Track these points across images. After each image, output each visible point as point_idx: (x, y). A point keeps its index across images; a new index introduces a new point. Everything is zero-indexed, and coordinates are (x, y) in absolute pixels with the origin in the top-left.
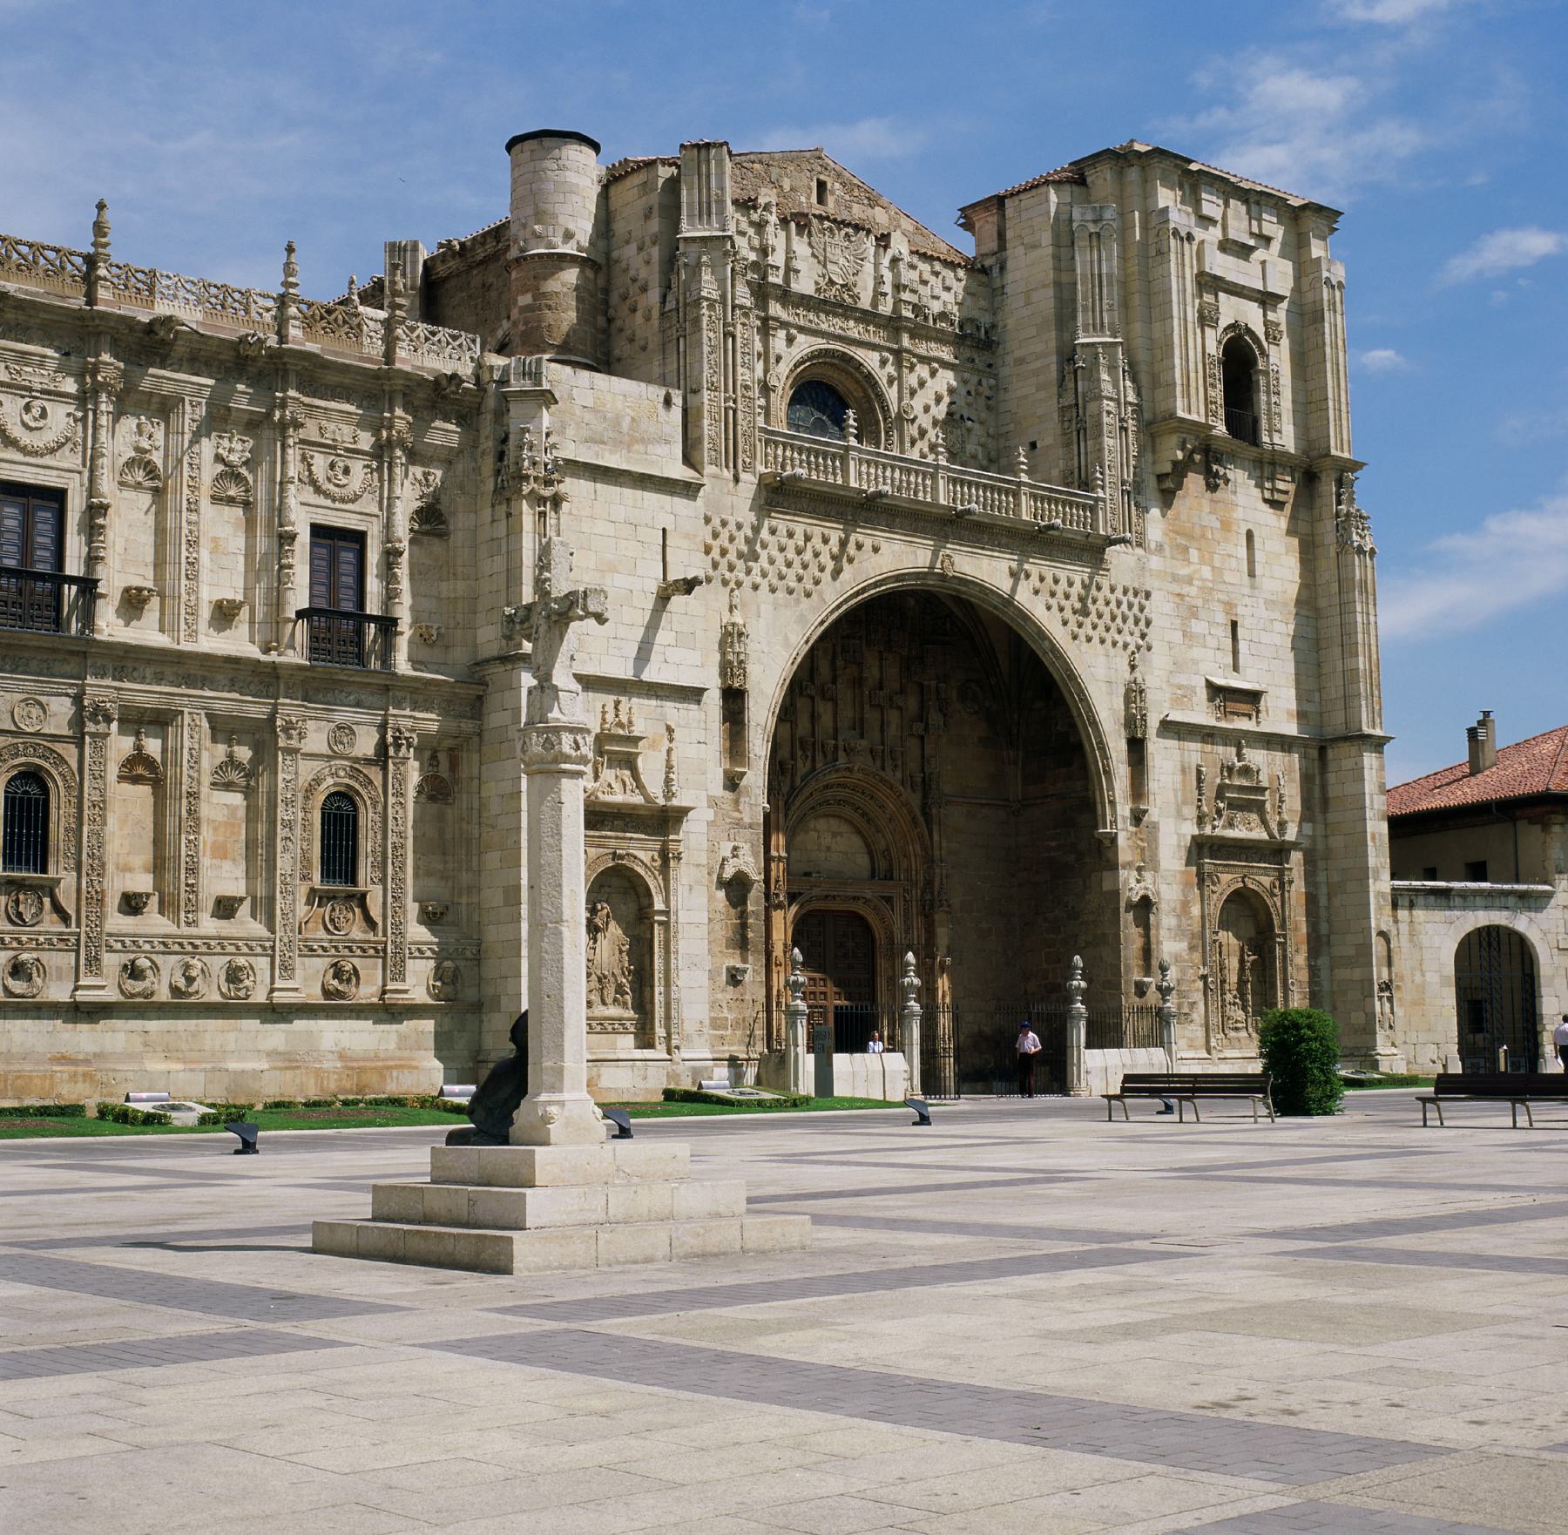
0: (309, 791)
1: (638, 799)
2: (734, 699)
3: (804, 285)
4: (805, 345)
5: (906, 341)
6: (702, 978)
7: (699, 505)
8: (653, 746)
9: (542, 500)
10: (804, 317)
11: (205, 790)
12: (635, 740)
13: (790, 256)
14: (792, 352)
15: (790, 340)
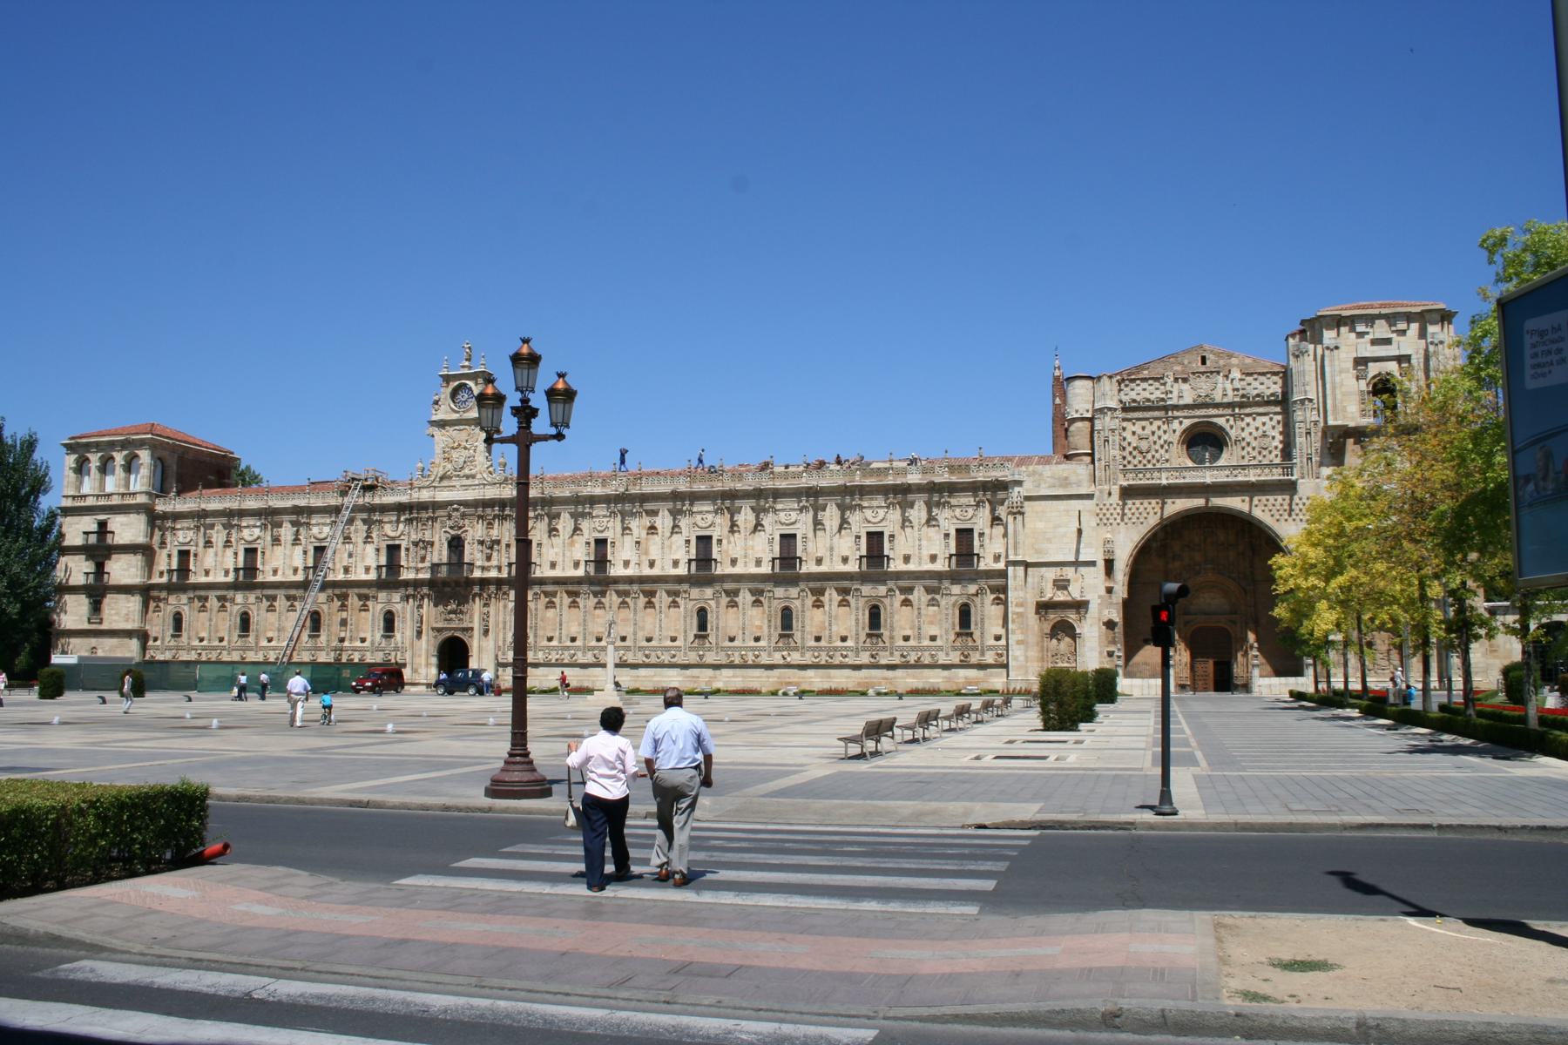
0: (954, 605)
1: (1069, 599)
2: (1109, 565)
3: (1188, 400)
4: (1187, 423)
5: (1237, 410)
6: (1096, 654)
7: (1094, 501)
8: (1076, 581)
9: (1015, 514)
10: (1185, 413)
11: (923, 607)
12: (1068, 581)
13: (1181, 391)
14: (1178, 427)
15: (1181, 423)
